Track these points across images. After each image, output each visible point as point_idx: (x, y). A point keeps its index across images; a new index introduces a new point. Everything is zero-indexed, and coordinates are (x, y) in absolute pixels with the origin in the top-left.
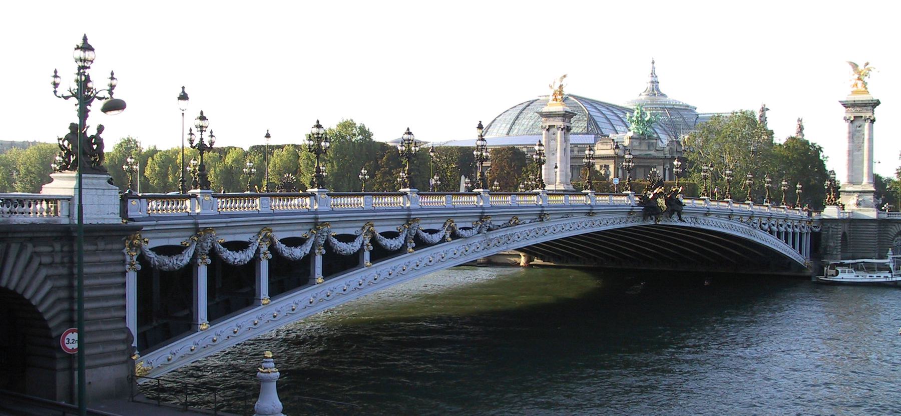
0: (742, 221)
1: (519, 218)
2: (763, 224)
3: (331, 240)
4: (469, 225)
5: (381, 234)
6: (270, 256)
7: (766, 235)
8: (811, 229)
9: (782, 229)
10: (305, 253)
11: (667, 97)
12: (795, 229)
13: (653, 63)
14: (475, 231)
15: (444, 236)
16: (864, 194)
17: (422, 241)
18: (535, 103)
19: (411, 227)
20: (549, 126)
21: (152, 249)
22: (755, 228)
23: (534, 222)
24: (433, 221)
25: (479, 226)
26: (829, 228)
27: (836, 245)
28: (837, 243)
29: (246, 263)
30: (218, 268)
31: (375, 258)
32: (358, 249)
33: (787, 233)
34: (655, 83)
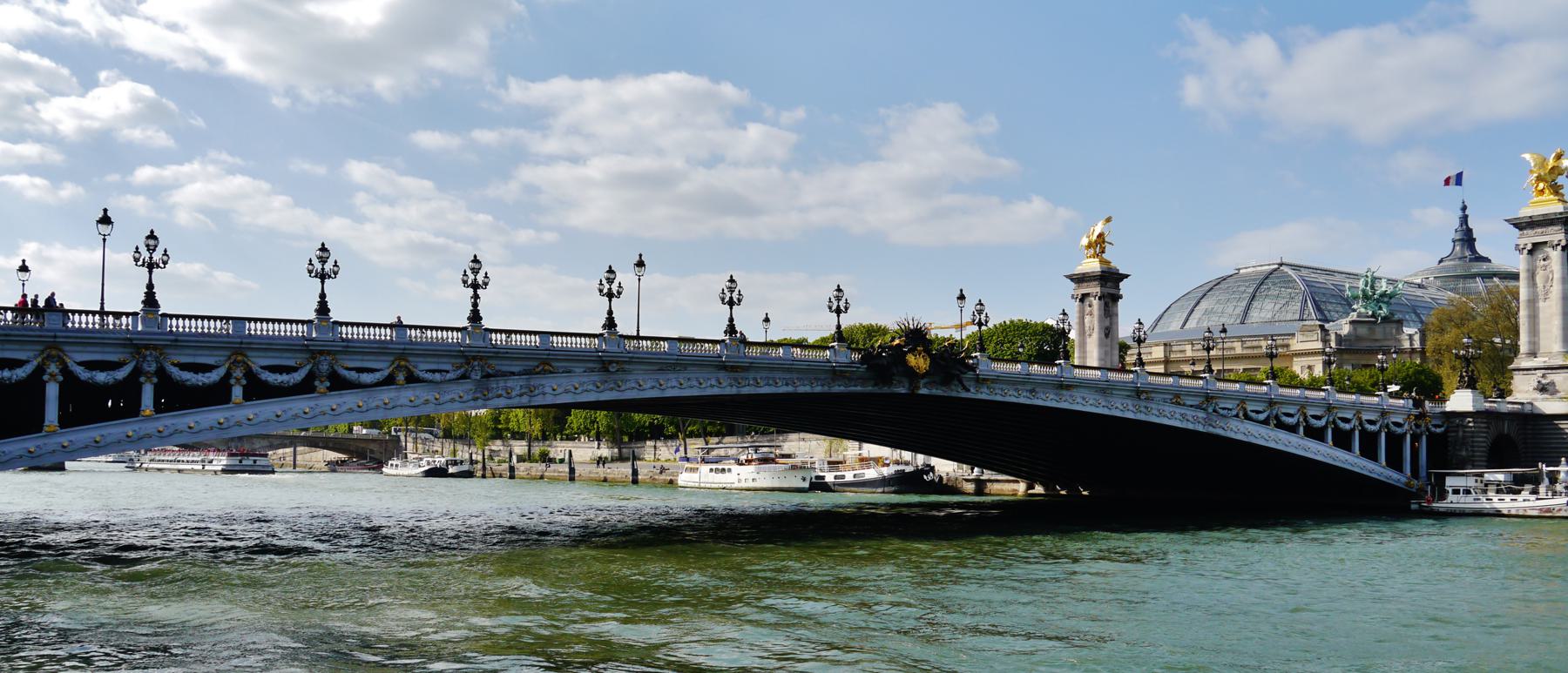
0: (1179, 404)
1: (554, 364)
2: (1253, 411)
6: (61, 378)
7: (1269, 432)
8: (1428, 429)
11: (1489, 261)
13: (1464, 208)
14: (449, 376)
16: (1554, 371)
18: (1229, 280)
19: (317, 360)
20: (1083, 295)
23: (593, 372)
24: (366, 358)
25: (462, 370)
27: (1471, 454)
28: (1473, 451)
31: (249, 396)
34: (1467, 238)
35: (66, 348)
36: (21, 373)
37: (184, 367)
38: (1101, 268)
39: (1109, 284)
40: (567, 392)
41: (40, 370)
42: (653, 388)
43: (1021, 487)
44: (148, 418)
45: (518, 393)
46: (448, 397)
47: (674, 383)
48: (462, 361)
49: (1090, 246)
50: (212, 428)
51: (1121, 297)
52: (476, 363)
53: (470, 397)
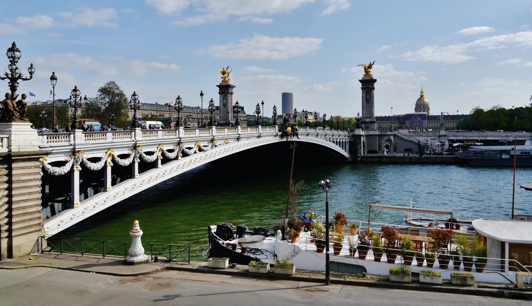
0: (321, 138)
3: (142, 155)
4: (207, 144)
5: (167, 150)
9: (338, 140)
10: (130, 162)
12: (343, 140)
15: (195, 151)
17: (185, 153)
21: (49, 164)
22: (327, 141)
26: (357, 139)
29: (100, 169)
30: (85, 172)
32: (156, 159)
33: (340, 142)
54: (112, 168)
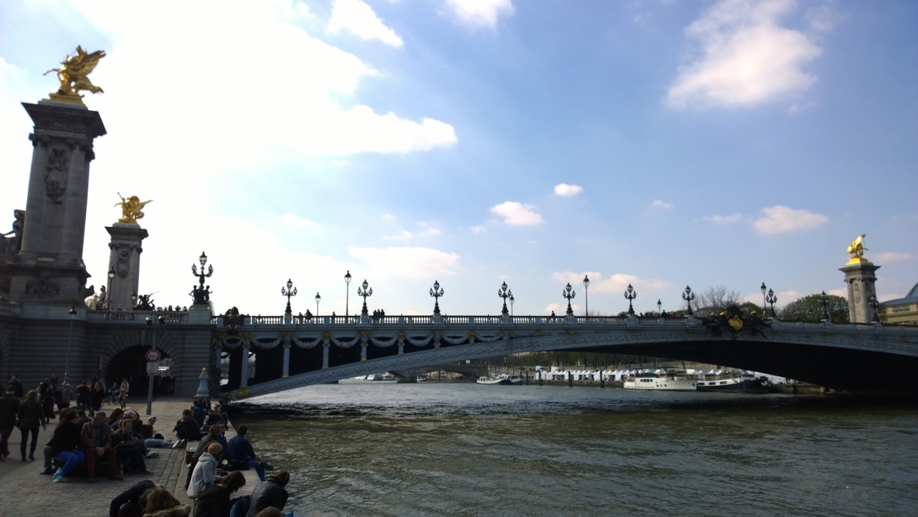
1: (544, 331)
6: (329, 346)
14: (494, 339)
25: (500, 336)
35: (332, 332)
36: (314, 344)
37: (379, 339)
38: (861, 263)
39: (868, 272)
40: (550, 344)
41: (321, 342)
42: (592, 341)
43: (822, 390)
44: (364, 362)
45: (527, 346)
46: (494, 349)
47: (603, 339)
48: (500, 331)
49: (853, 252)
50: (390, 365)
51: (876, 279)
52: (506, 332)
53: (504, 349)
54: (330, 349)
